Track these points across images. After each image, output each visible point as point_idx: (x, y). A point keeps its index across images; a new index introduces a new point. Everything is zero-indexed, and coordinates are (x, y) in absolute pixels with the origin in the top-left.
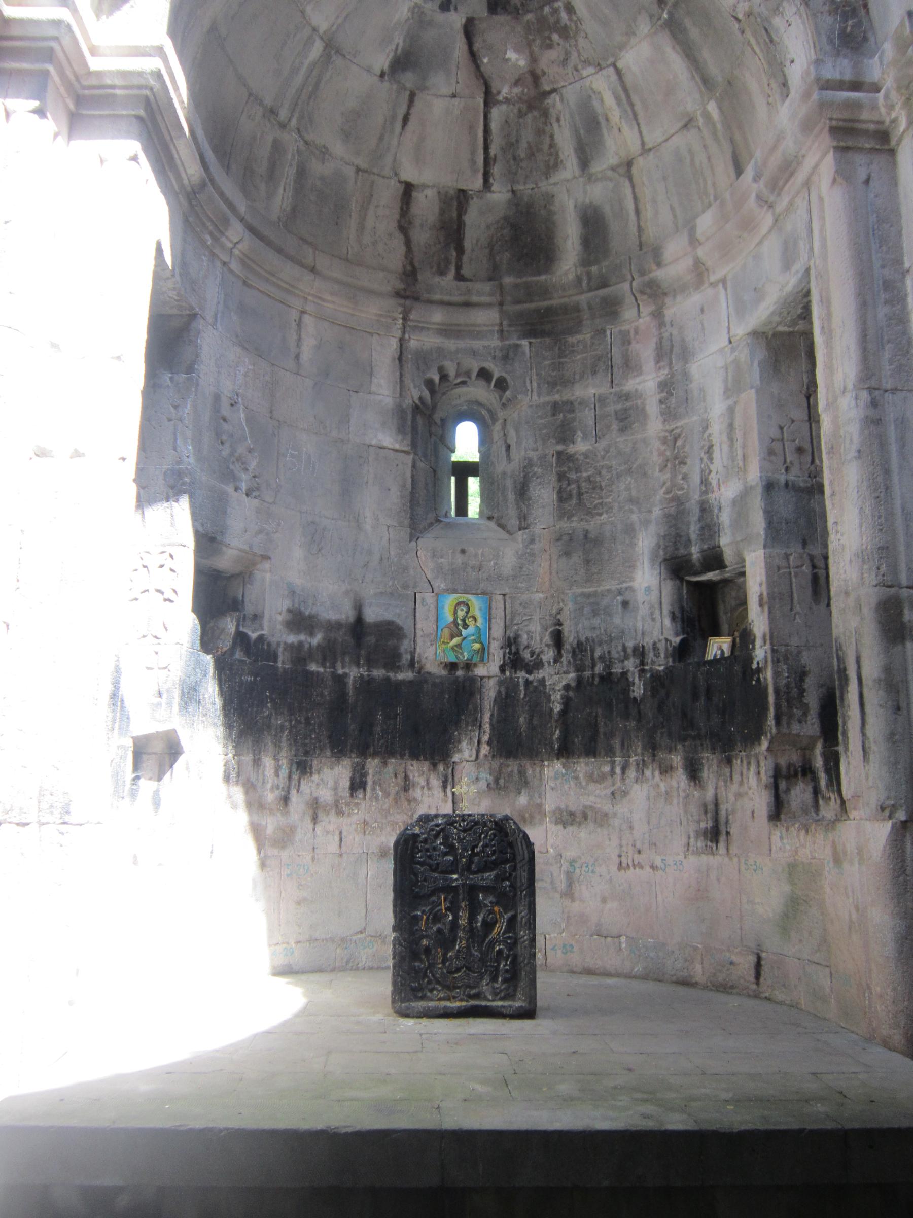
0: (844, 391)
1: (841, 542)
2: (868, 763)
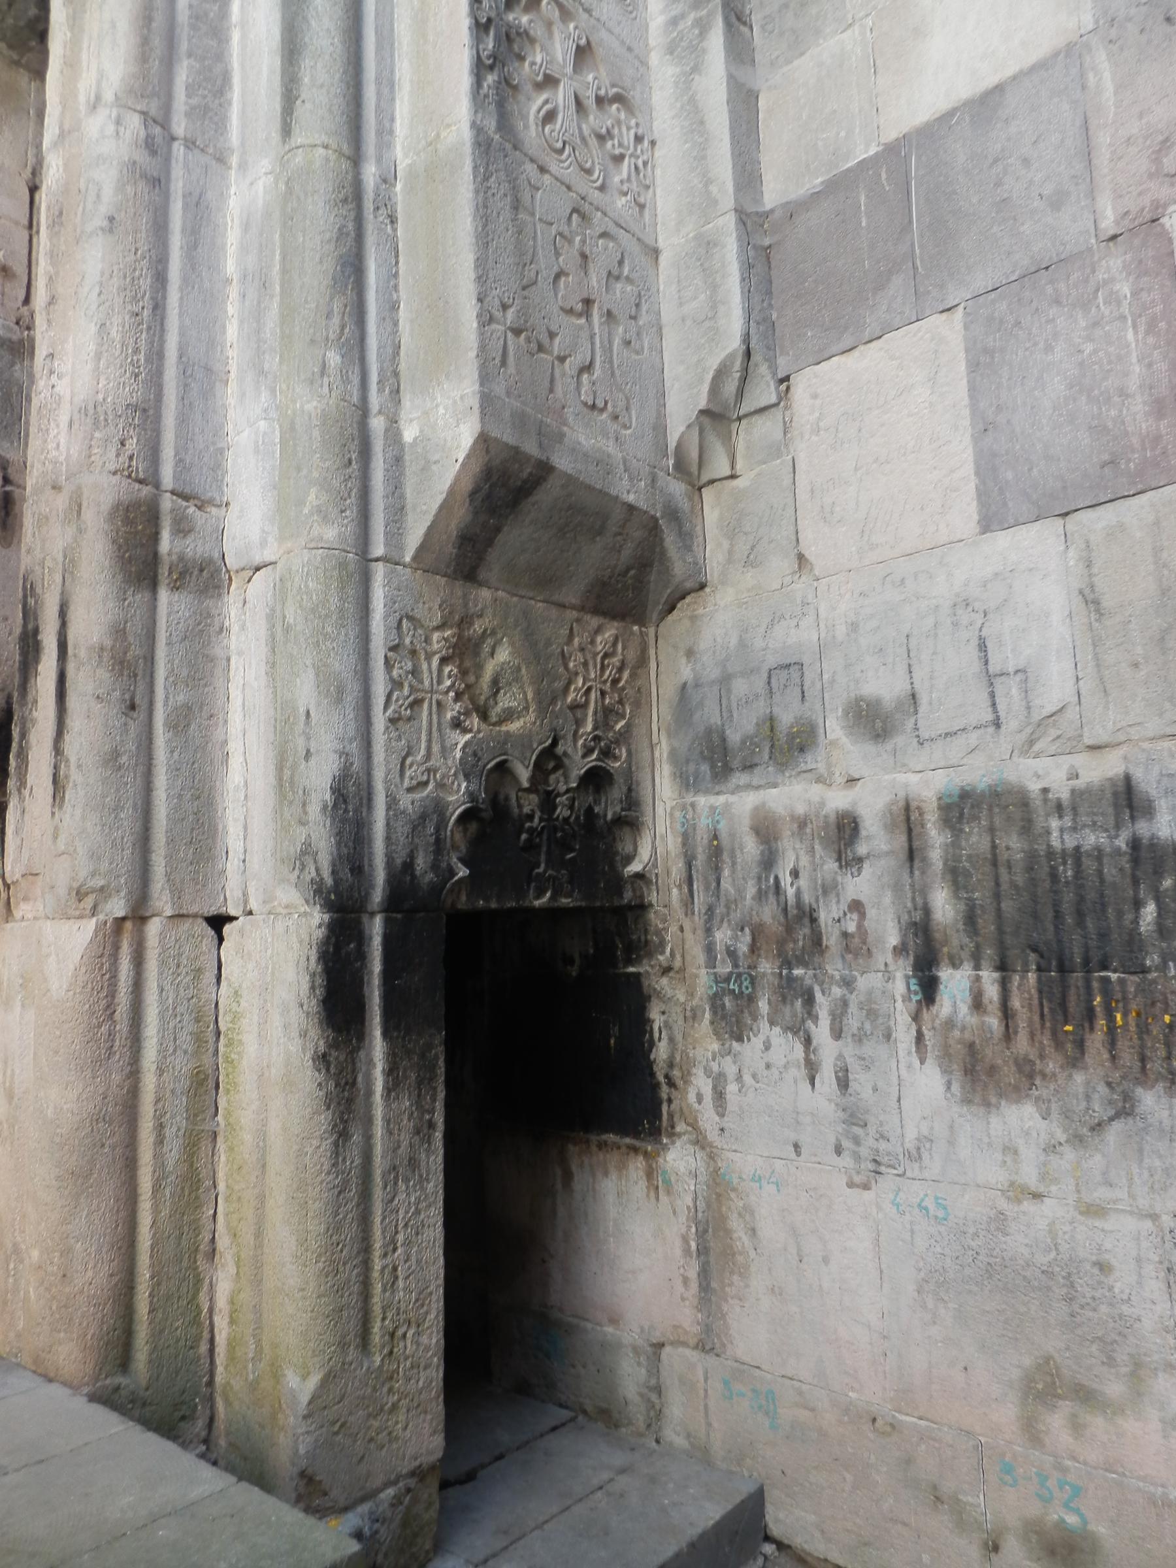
0: (95, 105)
1: (57, 389)
2: (61, 807)
